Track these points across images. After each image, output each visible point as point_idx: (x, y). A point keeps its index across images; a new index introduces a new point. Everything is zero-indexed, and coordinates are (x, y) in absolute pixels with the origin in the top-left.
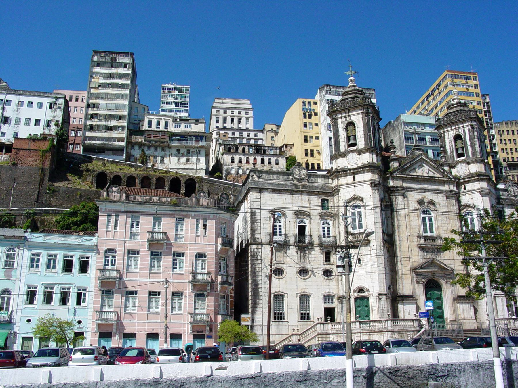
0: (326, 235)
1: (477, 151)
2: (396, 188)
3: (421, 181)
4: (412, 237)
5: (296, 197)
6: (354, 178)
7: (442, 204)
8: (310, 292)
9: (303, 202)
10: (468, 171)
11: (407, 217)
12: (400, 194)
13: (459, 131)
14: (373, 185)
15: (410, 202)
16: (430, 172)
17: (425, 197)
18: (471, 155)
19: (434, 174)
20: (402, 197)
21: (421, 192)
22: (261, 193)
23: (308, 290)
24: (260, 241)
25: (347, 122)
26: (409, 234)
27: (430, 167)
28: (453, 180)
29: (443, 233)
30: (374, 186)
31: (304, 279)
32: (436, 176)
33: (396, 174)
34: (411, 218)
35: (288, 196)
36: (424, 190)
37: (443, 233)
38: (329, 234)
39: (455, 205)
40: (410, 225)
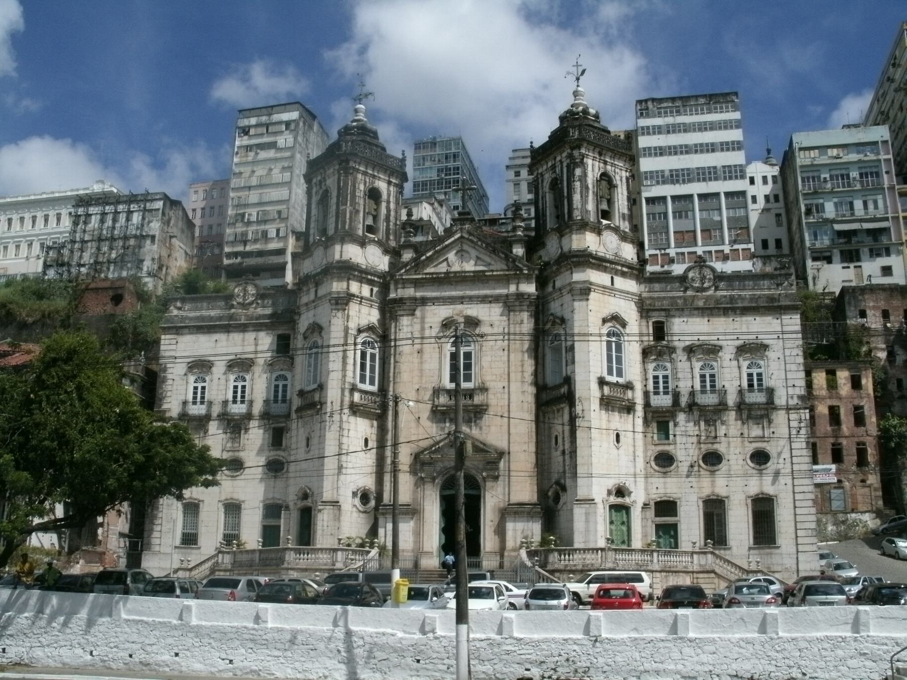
0: (239, 398)
1: (575, 207)
2: (400, 301)
3: (456, 282)
4: (422, 392)
5: (236, 337)
6: (316, 291)
7: (497, 323)
8: (242, 498)
9: (246, 343)
10: (560, 251)
11: (416, 354)
12: (408, 312)
13: (555, 172)
14: (333, 302)
15: (427, 326)
16: (479, 262)
17: (461, 312)
18: (566, 216)
19: (490, 264)
20: (410, 318)
21: (452, 303)
22: (177, 334)
23: (239, 496)
24: (168, 415)
25: (321, 192)
26: (417, 387)
27: (480, 252)
28: (526, 272)
29: (492, 381)
30: (337, 304)
31: (232, 477)
32: (492, 268)
33: (402, 275)
34: (426, 356)
35: (221, 337)
36: (461, 300)
37: (492, 381)
38: (243, 397)
39: (525, 321)
40: (421, 370)
